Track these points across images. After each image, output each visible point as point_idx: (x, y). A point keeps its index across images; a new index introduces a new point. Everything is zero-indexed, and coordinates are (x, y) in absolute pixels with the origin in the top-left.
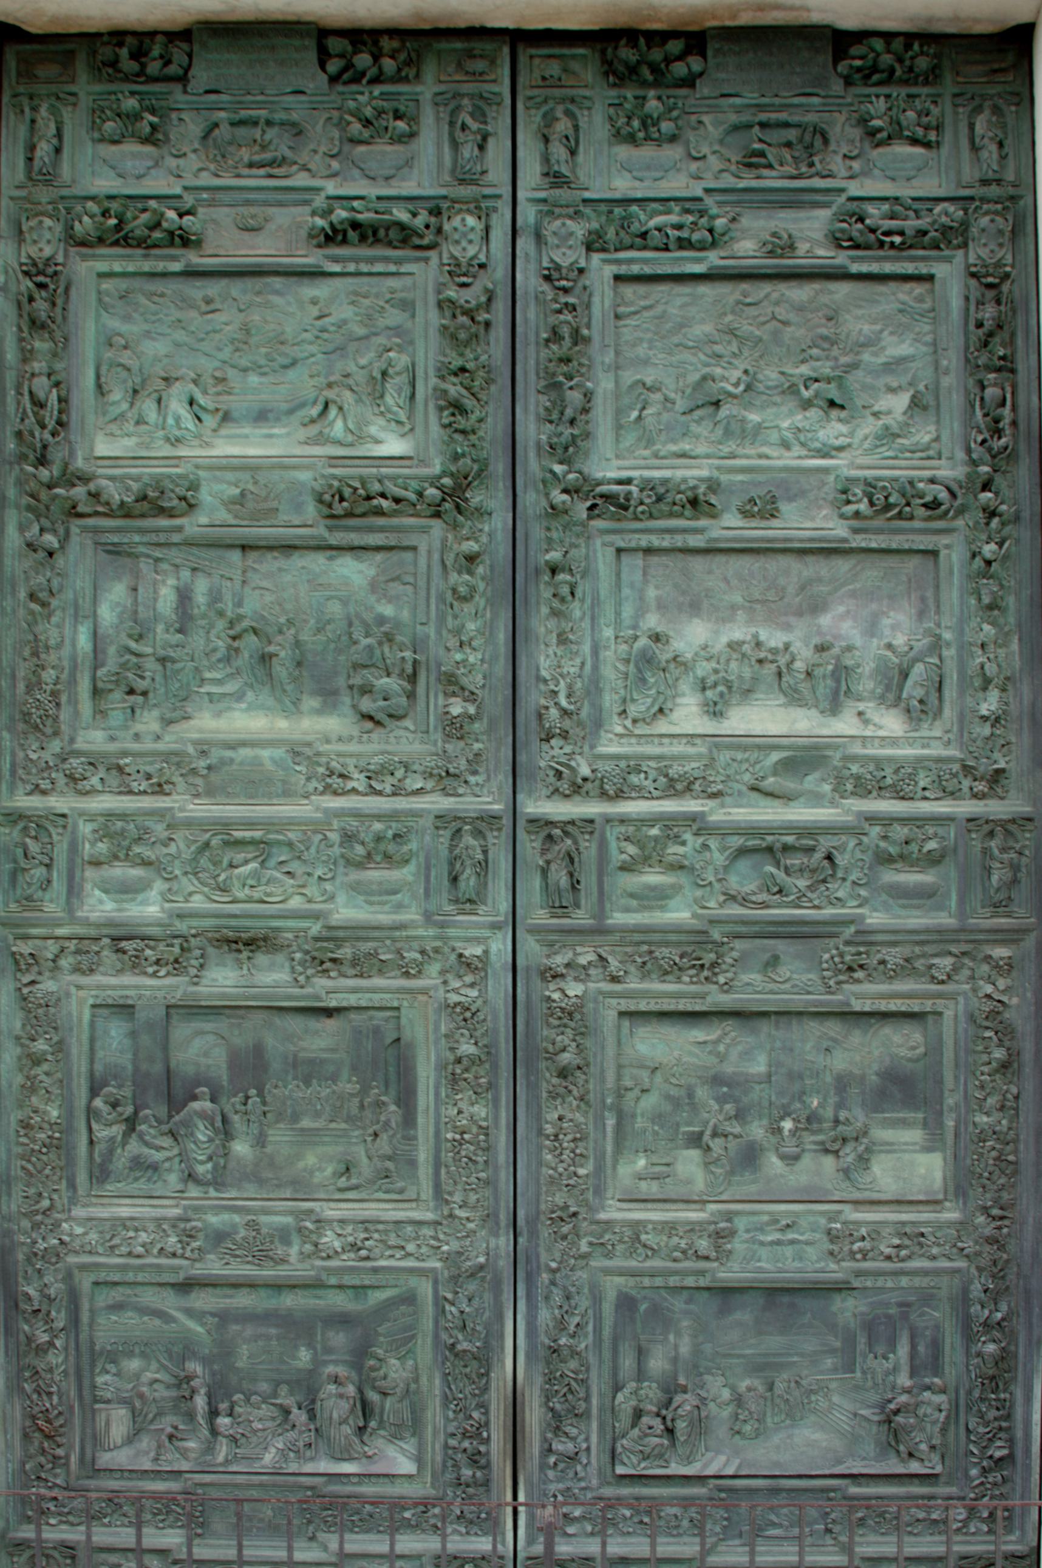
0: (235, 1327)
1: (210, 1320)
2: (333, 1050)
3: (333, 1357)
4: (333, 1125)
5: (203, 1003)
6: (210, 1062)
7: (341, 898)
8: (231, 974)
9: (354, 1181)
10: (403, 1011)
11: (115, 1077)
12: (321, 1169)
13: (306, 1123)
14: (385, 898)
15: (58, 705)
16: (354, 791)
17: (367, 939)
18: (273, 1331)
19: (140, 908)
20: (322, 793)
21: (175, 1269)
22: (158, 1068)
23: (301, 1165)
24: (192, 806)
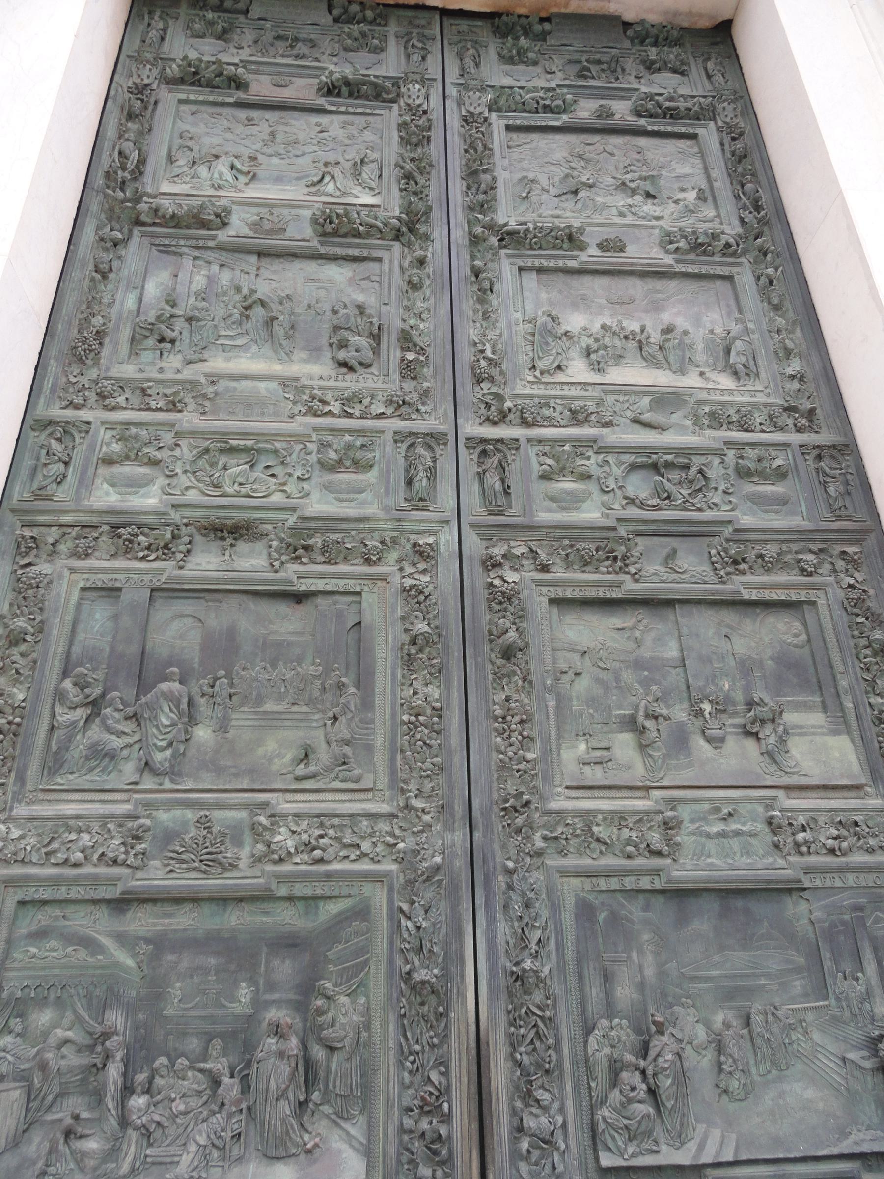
0: (171, 958)
1: (144, 948)
3: (276, 996)
18: (212, 961)
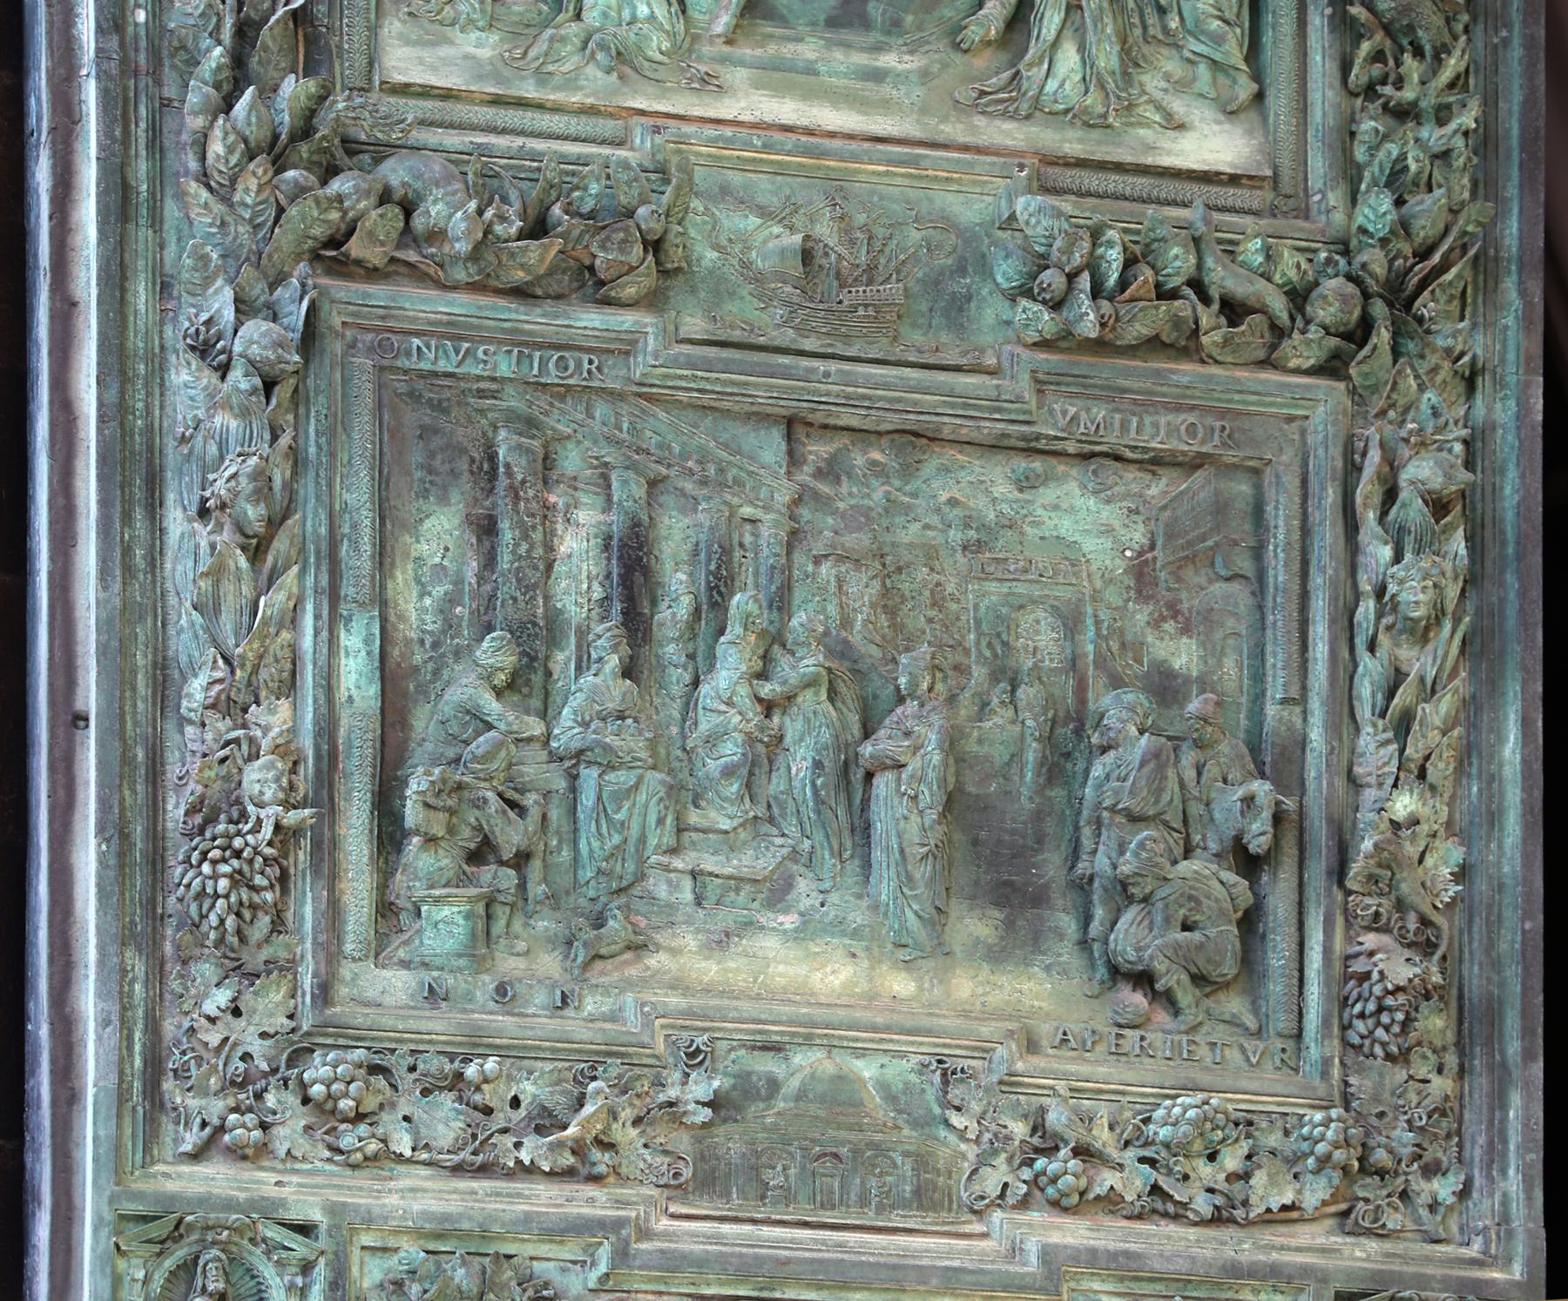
15: (284, 878)
16: (1111, 1202)
20: (1024, 1204)
24: (664, 1223)
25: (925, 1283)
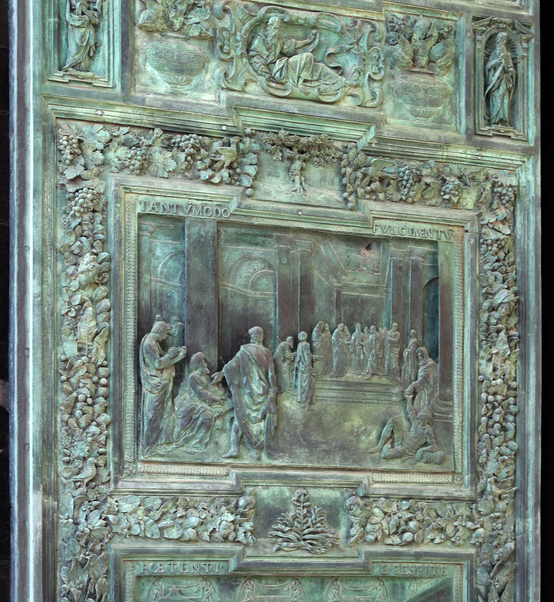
2: (373, 289)
4: (375, 380)
5: (255, 221)
6: (258, 295)
7: (389, 106)
8: (284, 188)
9: (398, 448)
10: (441, 246)
11: (161, 309)
12: (367, 433)
13: (351, 375)
14: (429, 109)
17: (410, 157)
19: (195, 94)
21: (225, 556)
22: (208, 300)
23: (347, 426)
25: (336, 4)
